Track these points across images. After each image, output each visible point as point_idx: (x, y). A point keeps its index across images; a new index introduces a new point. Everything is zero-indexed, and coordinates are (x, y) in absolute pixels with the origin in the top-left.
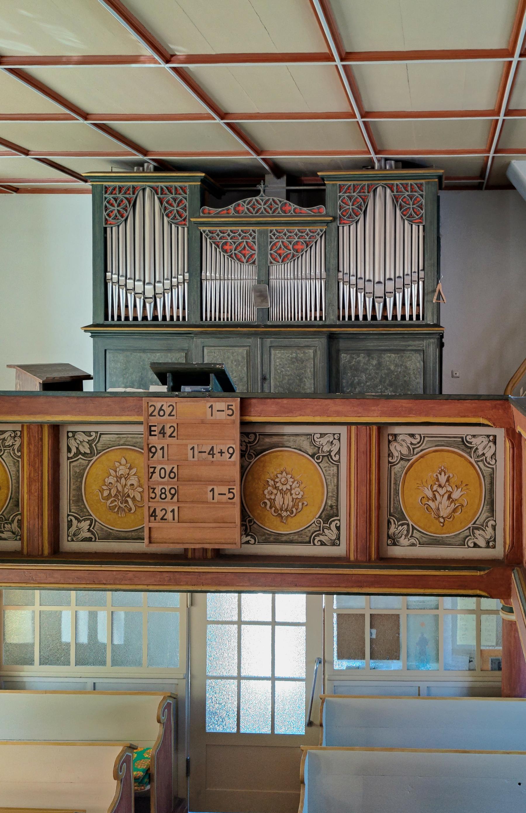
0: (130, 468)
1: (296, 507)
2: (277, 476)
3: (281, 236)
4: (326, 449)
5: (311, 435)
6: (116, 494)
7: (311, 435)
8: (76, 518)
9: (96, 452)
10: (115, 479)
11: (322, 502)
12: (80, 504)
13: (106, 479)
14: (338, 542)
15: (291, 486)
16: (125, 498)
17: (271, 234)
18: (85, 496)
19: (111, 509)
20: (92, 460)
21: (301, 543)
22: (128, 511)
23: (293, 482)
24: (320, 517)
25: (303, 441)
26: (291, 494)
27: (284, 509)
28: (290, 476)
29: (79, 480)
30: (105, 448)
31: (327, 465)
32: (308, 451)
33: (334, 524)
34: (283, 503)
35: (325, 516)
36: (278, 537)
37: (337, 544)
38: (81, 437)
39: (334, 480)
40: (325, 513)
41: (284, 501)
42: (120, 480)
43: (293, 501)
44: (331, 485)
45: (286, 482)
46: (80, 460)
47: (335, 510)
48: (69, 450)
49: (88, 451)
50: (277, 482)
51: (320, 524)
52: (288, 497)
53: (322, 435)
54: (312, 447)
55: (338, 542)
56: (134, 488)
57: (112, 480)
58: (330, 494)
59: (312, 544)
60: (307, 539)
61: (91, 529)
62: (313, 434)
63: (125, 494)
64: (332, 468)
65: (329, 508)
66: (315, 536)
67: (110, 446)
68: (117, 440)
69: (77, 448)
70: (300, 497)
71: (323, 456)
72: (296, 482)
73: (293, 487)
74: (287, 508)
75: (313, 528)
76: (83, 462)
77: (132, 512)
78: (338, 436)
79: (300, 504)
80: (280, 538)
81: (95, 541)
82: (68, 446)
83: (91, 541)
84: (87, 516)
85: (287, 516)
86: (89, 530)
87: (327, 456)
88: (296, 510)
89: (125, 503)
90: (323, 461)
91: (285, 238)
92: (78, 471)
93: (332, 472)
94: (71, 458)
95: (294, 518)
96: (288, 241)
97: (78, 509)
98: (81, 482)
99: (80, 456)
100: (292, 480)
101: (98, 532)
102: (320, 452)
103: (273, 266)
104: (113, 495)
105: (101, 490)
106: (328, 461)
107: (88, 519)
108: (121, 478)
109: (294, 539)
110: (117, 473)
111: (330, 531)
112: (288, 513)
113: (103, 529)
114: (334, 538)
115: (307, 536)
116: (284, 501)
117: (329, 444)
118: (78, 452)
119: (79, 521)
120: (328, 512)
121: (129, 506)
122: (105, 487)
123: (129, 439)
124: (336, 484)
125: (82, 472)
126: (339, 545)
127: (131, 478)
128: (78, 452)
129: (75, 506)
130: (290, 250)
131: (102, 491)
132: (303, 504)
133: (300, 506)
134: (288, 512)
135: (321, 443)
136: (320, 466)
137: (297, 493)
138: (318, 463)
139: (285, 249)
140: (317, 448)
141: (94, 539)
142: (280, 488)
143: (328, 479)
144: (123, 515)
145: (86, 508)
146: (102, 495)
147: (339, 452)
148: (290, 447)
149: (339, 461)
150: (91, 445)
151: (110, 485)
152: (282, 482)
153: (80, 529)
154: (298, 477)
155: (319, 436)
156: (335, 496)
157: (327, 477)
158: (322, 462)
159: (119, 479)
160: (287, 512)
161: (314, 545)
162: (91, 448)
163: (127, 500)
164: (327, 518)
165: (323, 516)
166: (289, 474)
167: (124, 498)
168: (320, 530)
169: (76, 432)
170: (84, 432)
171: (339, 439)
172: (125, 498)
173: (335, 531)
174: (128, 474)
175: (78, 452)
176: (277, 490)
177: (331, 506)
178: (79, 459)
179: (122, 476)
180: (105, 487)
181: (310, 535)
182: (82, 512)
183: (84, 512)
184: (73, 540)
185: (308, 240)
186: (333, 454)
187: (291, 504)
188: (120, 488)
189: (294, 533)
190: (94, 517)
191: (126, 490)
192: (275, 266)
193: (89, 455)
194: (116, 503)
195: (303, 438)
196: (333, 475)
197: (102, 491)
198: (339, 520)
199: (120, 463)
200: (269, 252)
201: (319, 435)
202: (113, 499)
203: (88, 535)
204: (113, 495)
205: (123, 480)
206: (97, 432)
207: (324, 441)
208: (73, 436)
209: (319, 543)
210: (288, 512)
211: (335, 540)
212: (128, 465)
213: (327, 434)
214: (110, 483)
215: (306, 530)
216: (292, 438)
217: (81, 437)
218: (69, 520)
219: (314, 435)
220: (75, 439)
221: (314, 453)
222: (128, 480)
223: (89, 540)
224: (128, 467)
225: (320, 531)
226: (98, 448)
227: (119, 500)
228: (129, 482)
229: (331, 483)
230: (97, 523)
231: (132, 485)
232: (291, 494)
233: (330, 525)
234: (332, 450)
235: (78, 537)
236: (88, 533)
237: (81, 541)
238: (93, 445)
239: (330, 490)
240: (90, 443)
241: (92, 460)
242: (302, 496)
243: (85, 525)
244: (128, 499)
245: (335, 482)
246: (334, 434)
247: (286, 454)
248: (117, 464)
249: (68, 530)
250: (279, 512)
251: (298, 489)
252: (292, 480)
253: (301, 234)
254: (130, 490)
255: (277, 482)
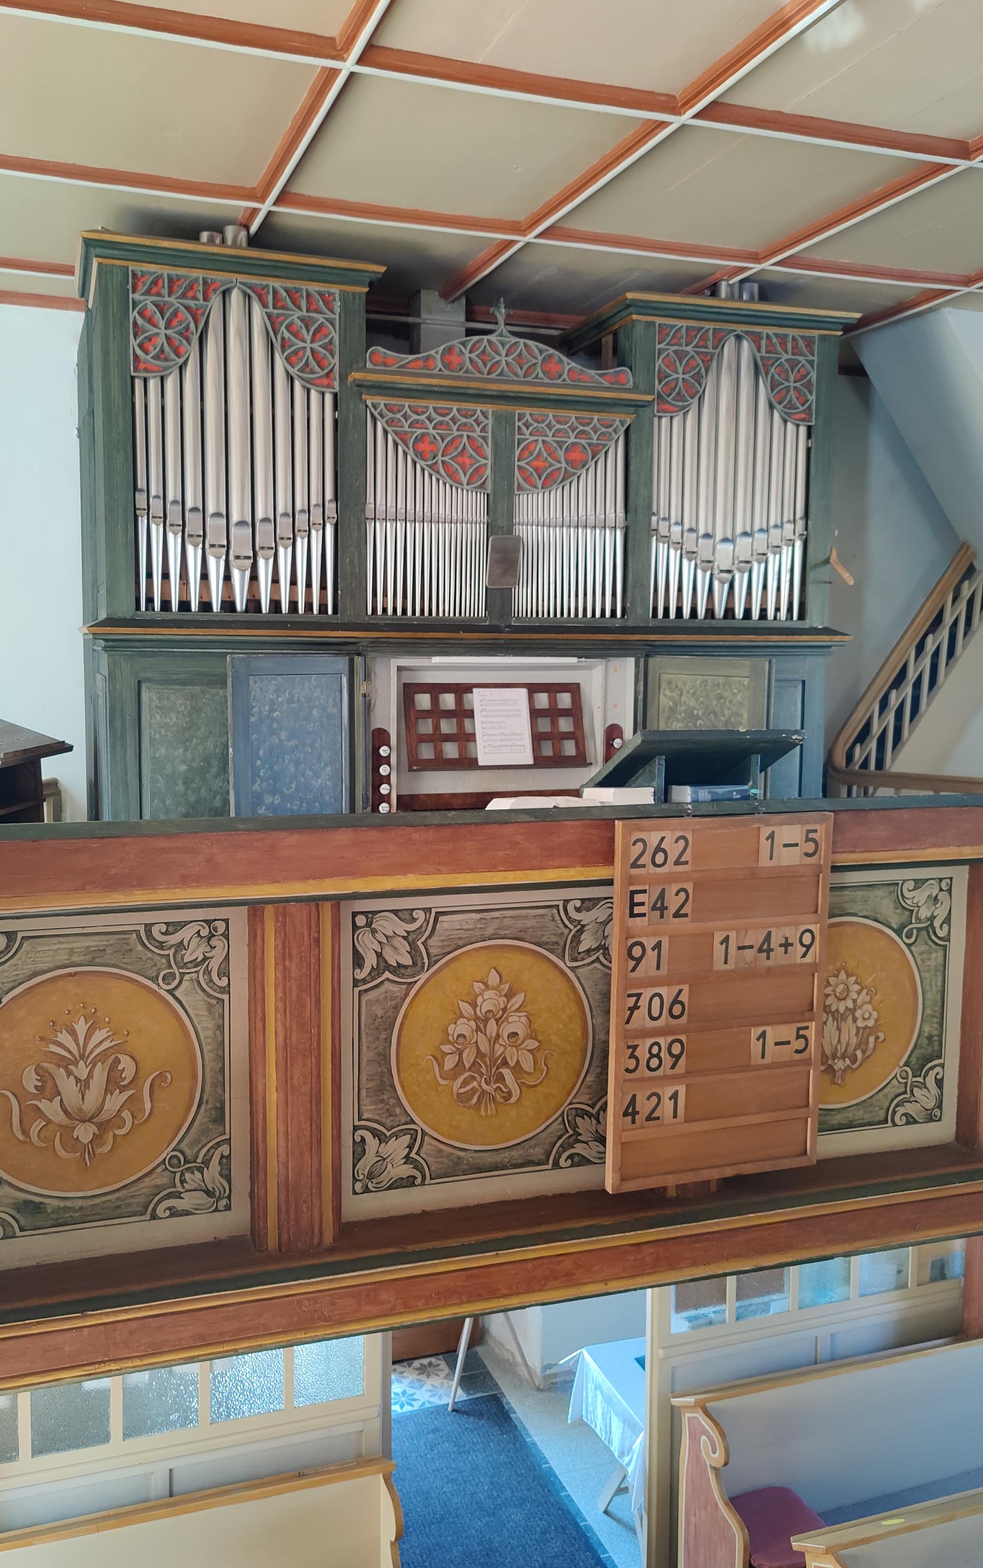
0: (510, 995)
1: (863, 1047)
2: (828, 982)
4: (924, 913)
5: (898, 884)
6: (475, 1061)
7: (898, 884)
8: (375, 1133)
9: (426, 960)
10: (473, 1024)
11: (912, 1032)
12: (385, 1097)
13: (451, 1029)
14: (938, 1113)
15: (854, 1001)
16: (497, 1069)
18: (399, 1077)
19: (463, 1099)
20: (416, 982)
21: (870, 1124)
22: (501, 1100)
23: (859, 993)
24: (907, 1064)
25: (883, 897)
26: (855, 1020)
27: (839, 1055)
28: (853, 979)
29: (383, 1036)
30: (449, 949)
31: (924, 948)
32: (890, 919)
33: (932, 1074)
34: (839, 1042)
35: (918, 1059)
36: (825, 1119)
37: (936, 1117)
38: (388, 925)
39: (936, 981)
40: (918, 1052)
41: (839, 1037)
42: (485, 1026)
43: (857, 1035)
44: (931, 990)
45: (845, 994)
46: (387, 985)
47: (936, 1044)
48: (358, 961)
49: (407, 961)
50: (828, 995)
51: (907, 1078)
52: (849, 1028)
53: (919, 883)
54: (899, 911)
55: (938, 1114)
56: (519, 1042)
57: (464, 1027)
58: (928, 1012)
59: (890, 1124)
60: (881, 1115)
61: (413, 1155)
62: (901, 883)
63: (498, 1059)
64: (934, 955)
65: (926, 1041)
66: (897, 1105)
67: (460, 943)
68: (478, 926)
69: (379, 955)
70: (871, 1023)
71: (919, 930)
72: (865, 992)
73: (859, 1002)
74: (846, 1050)
75: (896, 1088)
76: (395, 988)
77: (513, 1100)
78: (948, 884)
79: (872, 1039)
80: (828, 1118)
81: (423, 1184)
82: (355, 951)
83: (413, 1184)
84: (404, 1124)
85: (845, 1068)
86: (407, 1158)
87: (926, 928)
88: (864, 1052)
89: (496, 1081)
90: (919, 940)
92: (380, 1013)
93: (932, 963)
94: (364, 981)
95: (858, 1071)
97: (380, 1109)
98: (388, 1040)
99: (387, 975)
100: (857, 987)
101: (430, 1160)
102: (913, 921)
104: (467, 1066)
105: (439, 1056)
106: (926, 937)
107: (405, 1132)
108: (486, 1021)
109: (857, 1117)
110: (478, 1009)
111: (924, 1091)
112: (848, 1061)
113: (440, 1151)
114: (931, 1104)
115: (882, 1109)
116: (839, 1037)
117: (931, 902)
118: (382, 965)
119: (382, 1139)
120: (923, 1051)
121: (506, 1086)
122: (446, 1048)
123: (507, 922)
124: (940, 988)
125: (390, 1014)
126: (940, 1120)
127: (510, 1019)
128: (383, 965)
129: (373, 1103)
131: (439, 1058)
132: (877, 1038)
133: (871, 1045)
134: (847, 1059)
135: (915, 901)
136: (911, 952)
137: (867, 1016)
138: (909, 946)
140: (907, 913)
141: (419, 1180)
142: (833, 1009)
143: (925, 978)
144: (491, 1108)
145: (401, 1105)
146: (441, 1066)
147: (948, 920)
148: (855, 915)
149: (947, 939)
150: (412, 944)
151: (461, 1040)
152: (838, 995)
153: (384, 1159)
154: (868, 981)
155: (911, 885)
156: (938, 1015)
157: (925, 975)
158: (917, 943)
159: (481, 1022)
160: (844, 1060)
161: (895, 1125)
162: (414, 950)
163: (501, 1073)
164: (920, 1065)
165: (914, 1060)
166: (853, 975)
167: (493, 1071)
168: (905, 1092)
169: (375, 913)
170: (395, 912)
171: (950, 891)
172: (497, 1069)
173: (934, 1090)
174: (505, 1010)
175: (383, 965)
176: (827, 1013)
177: (930, 1038)
178: (382, 982)
179: (490, 1015)
180: (446, 1048)
181: (886, 1105)
182: (391, 1115)
183: (396, 1115)
184: (366, 1190)
186: (937, 923)
187: (854, 1041)
188: (484, 1047)
189: (857, 1104)
190: (420, 1124)
191: (499, 1050)
193: (409, 970)
194: (475, 1084)
195: (879, 893)
196: (936, 970)
197: (439, 1058)
198: (942, 1066)
199: (486, 984)
201: (912, 882)
202: (467, 1074)
203: (407, 1170)
204: (467, 1066)
205: (492, 1026)
206: (427, 910)
207: (920, 896)
208: (369, 924)
209: (904, 1118)
210: (847, 1059)
211: (933, 1109)
212: (506, 987)
213: (928, 880)
214: (459, 1036)
215: (880, 1094)
216: (860, 893)
217: (388, 925)
218: (358, 1139)
219: (903, 884)
220: (374, 932)
221: (902, 924)
222: (504, 1024)
223: (409, 1182)
224: (504, 993)
225: (906, 1094)
226: (431, 951)
227: (481, 1074)
228: (507, 1030)
229: (931, 986)
230: (426, 1138)
231: (514, 1035)
232: (855, 1020)
233: (924, 1078)
234: (935, 915)
235: (379, 1179)
236: (407, 1166)
237: (387, 1189)
238: (419, 943)
239: (928, 1003)
240: (410, 939)
241: (416, 982)
242: (876, 1021)
243: (397, 1147)
244: (506, 1072)
245: (939, 984)
246: (941, 880)
247: (849, 930)
248: (478, 987)
249: (354, 1167)
250: (830, 1062)
251: (869, 1007)
252: (857, 987)
254: (509, 1048)
255: (828, 995)
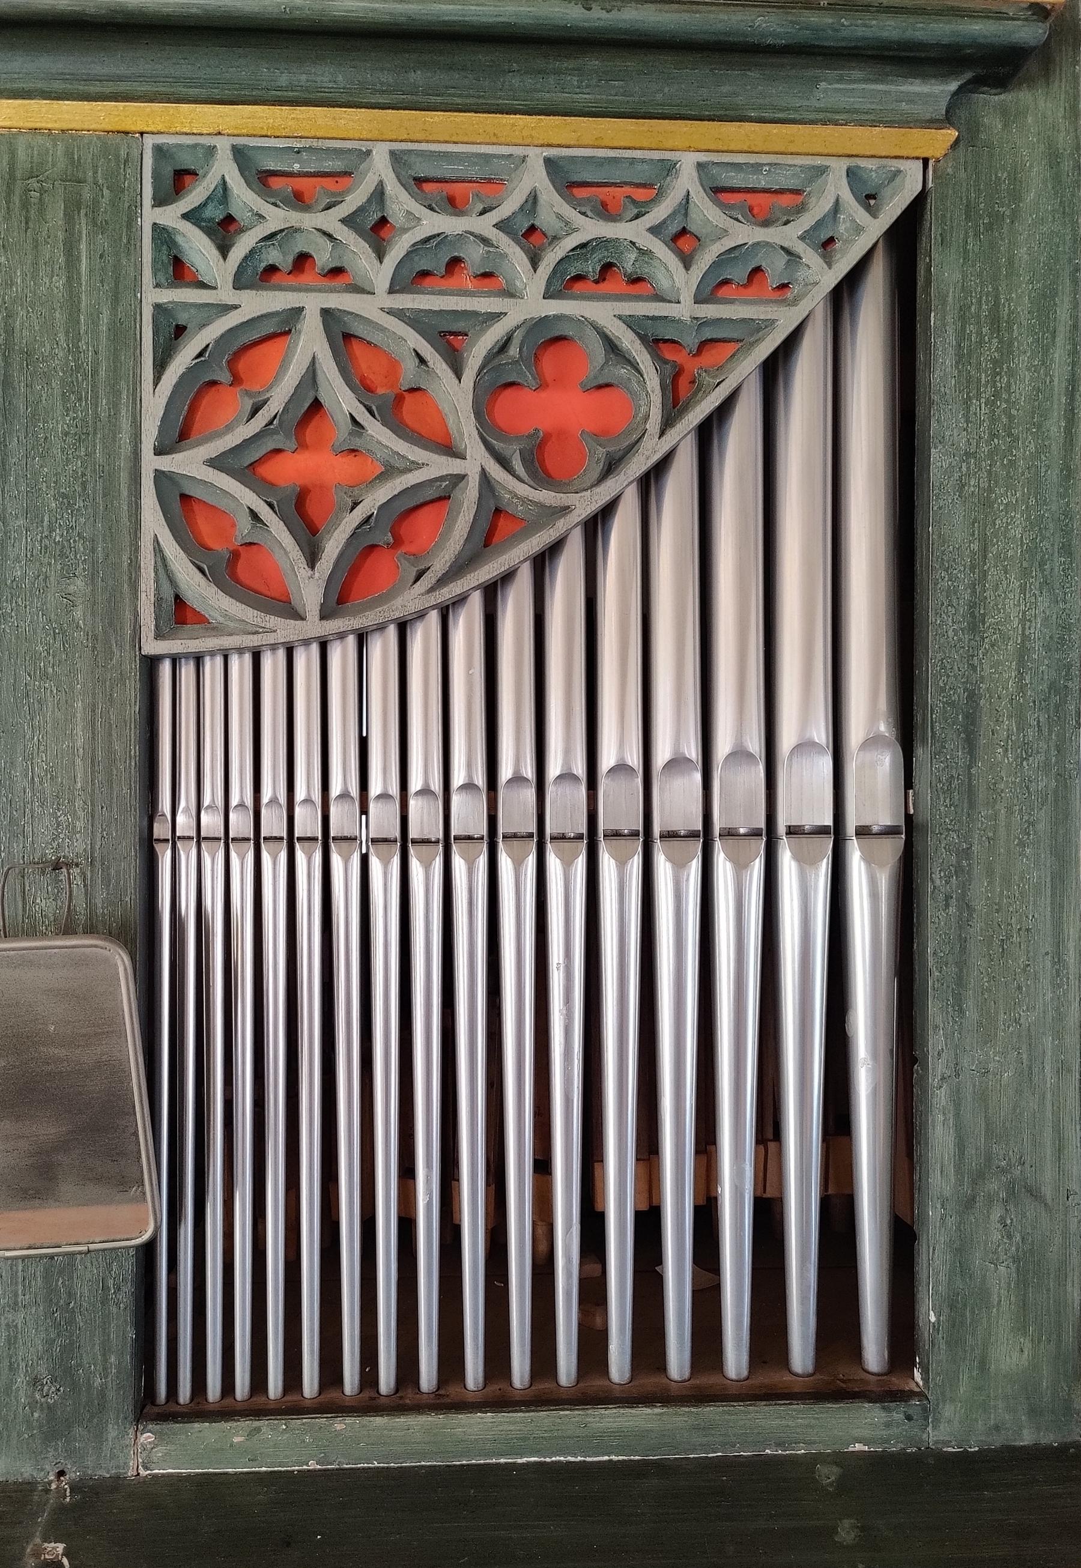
3: (323, 256)
17: (170, 216)
91: (381, 275)
96: (415, 320)
103: (212, 668)
130: (449, 449)
139: (375, 429)
185: (685, 310)
192: (240, 668)
200: (150, 463)
253: (591, 229)
